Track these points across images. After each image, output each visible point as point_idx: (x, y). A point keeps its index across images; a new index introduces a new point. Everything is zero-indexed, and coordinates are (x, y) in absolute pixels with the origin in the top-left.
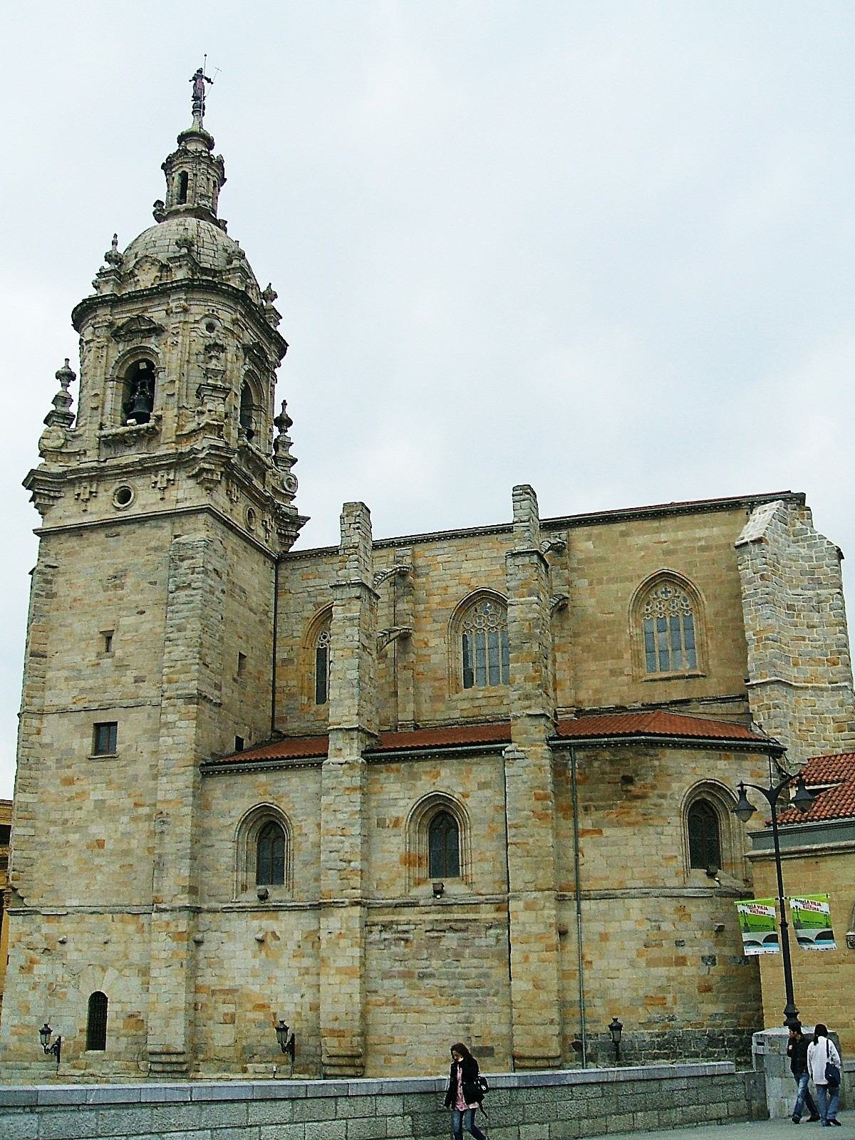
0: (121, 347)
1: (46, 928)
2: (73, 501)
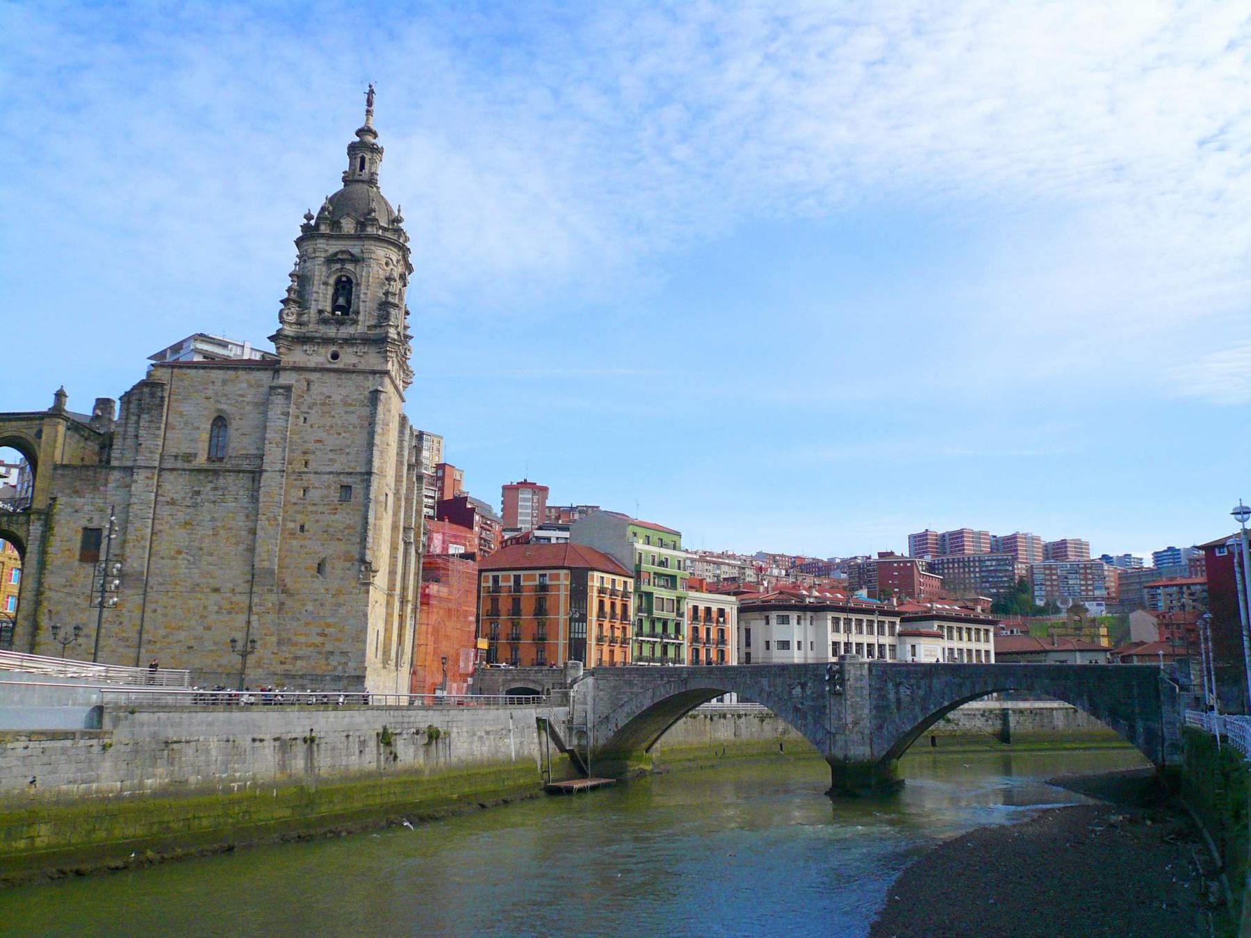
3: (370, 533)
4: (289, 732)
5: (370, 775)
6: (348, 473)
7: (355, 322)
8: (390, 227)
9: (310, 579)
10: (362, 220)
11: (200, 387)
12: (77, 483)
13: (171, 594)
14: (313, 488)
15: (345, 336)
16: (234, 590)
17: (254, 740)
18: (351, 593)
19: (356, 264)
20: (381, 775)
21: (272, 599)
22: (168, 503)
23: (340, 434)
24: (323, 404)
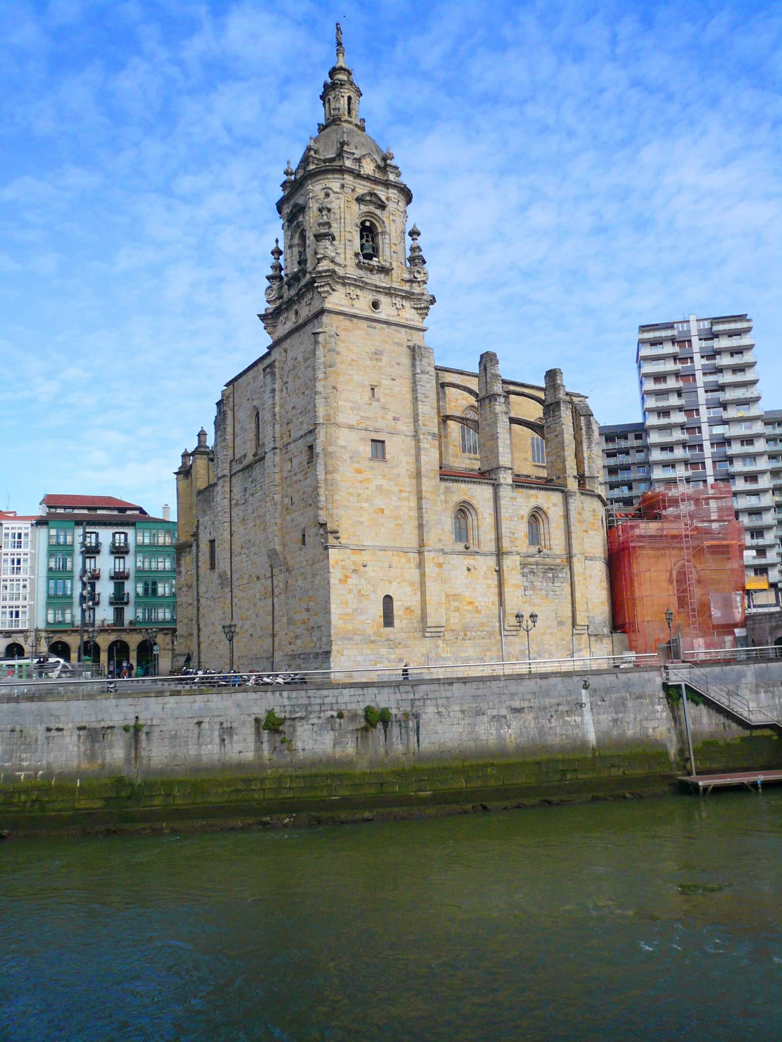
0: (362, 207)
1: (354, 558)
2: (344, 296)
3: (322, 491)
4: (103, 720)
5: (240, 766)
17: (49, 730)
20: (263, 767)
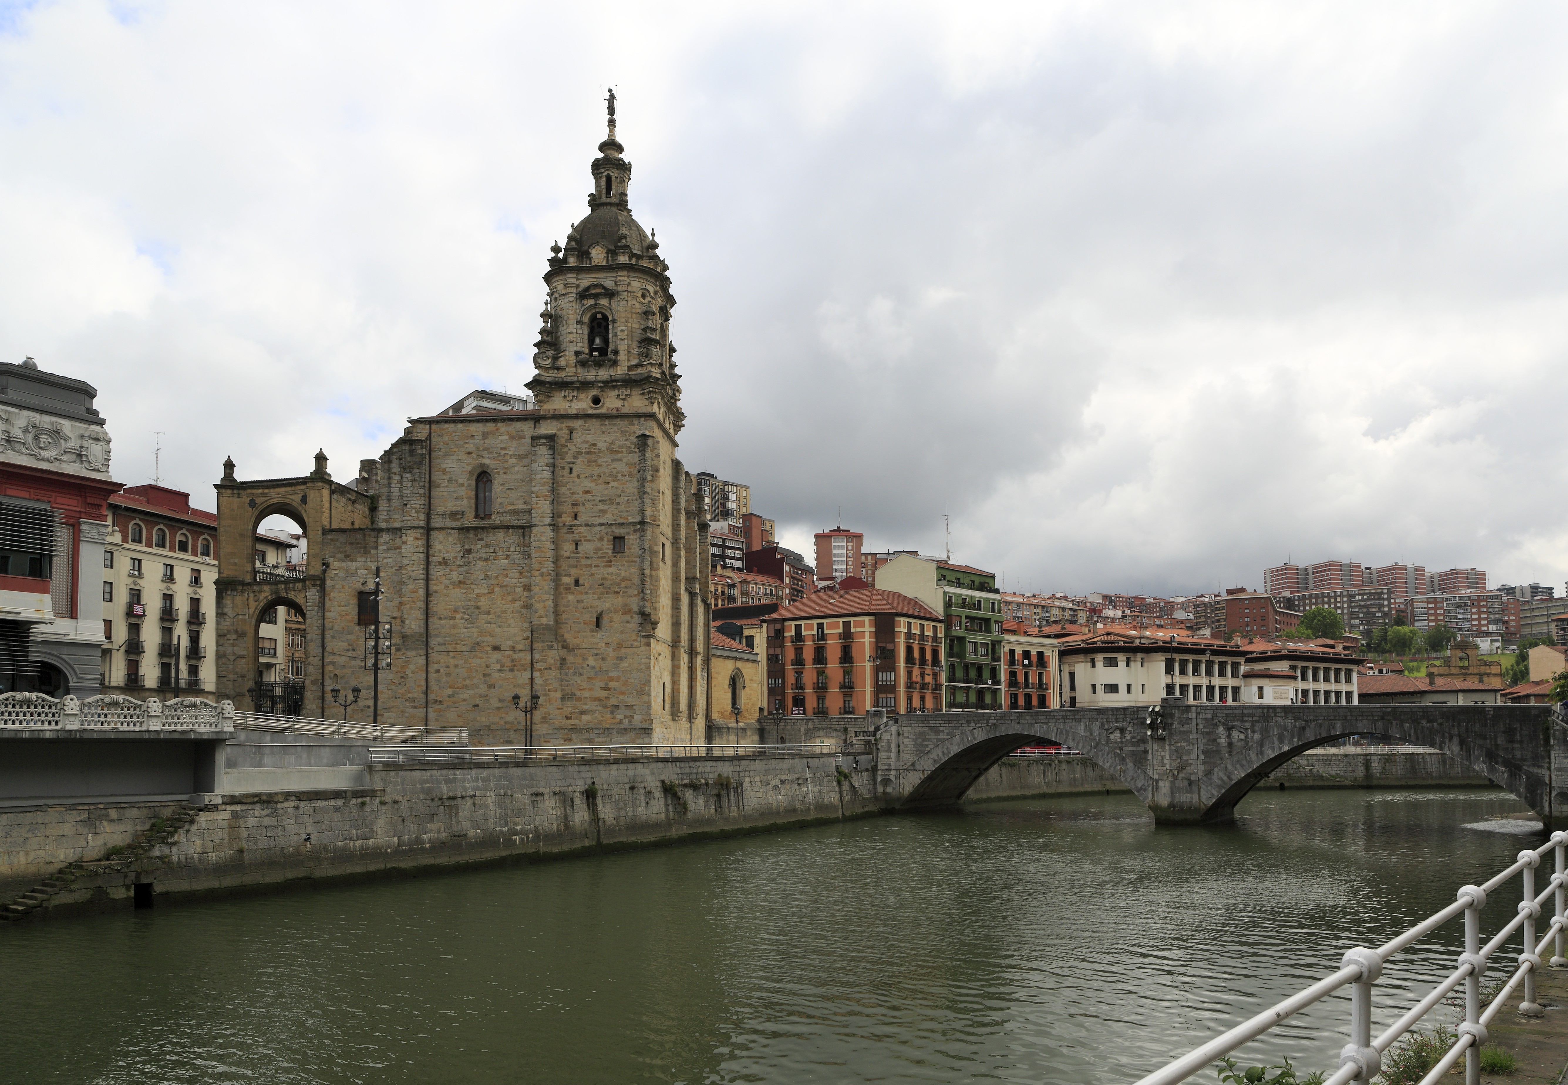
6: (619, 524)
7: (615, 363)
8: (645, 254)
9: (589, 634)
10: (613, 248)
11: (461, 443)
12: (348, 548)
13: (451, 654)
14: (586, 540)
15: (605, 378)
16: (514, 647)
18: (632, 646)
19: (610, 298)
21: (553, 655)
22: (440, 563)
23: (608, 483)
24: (589, 453)
